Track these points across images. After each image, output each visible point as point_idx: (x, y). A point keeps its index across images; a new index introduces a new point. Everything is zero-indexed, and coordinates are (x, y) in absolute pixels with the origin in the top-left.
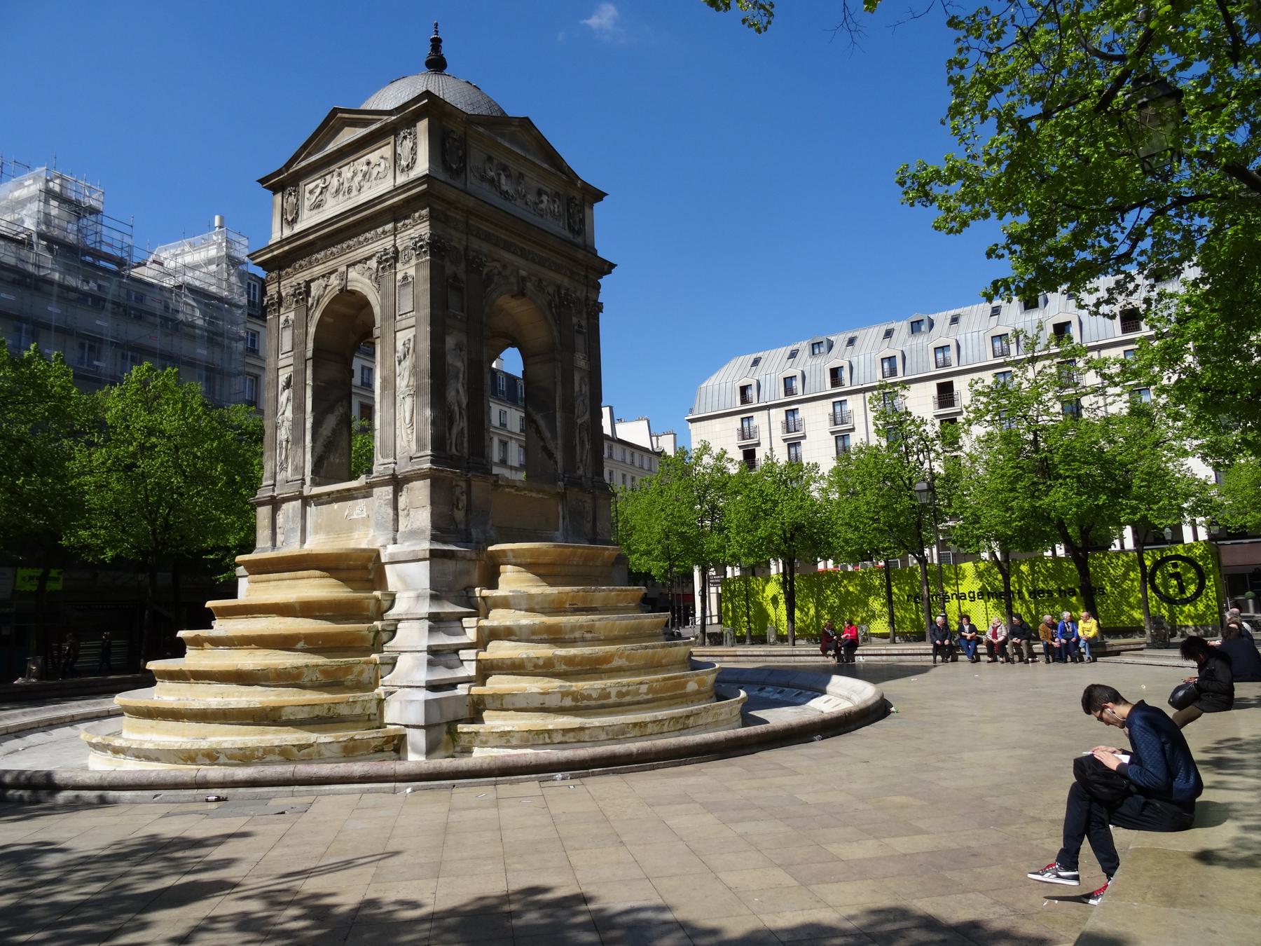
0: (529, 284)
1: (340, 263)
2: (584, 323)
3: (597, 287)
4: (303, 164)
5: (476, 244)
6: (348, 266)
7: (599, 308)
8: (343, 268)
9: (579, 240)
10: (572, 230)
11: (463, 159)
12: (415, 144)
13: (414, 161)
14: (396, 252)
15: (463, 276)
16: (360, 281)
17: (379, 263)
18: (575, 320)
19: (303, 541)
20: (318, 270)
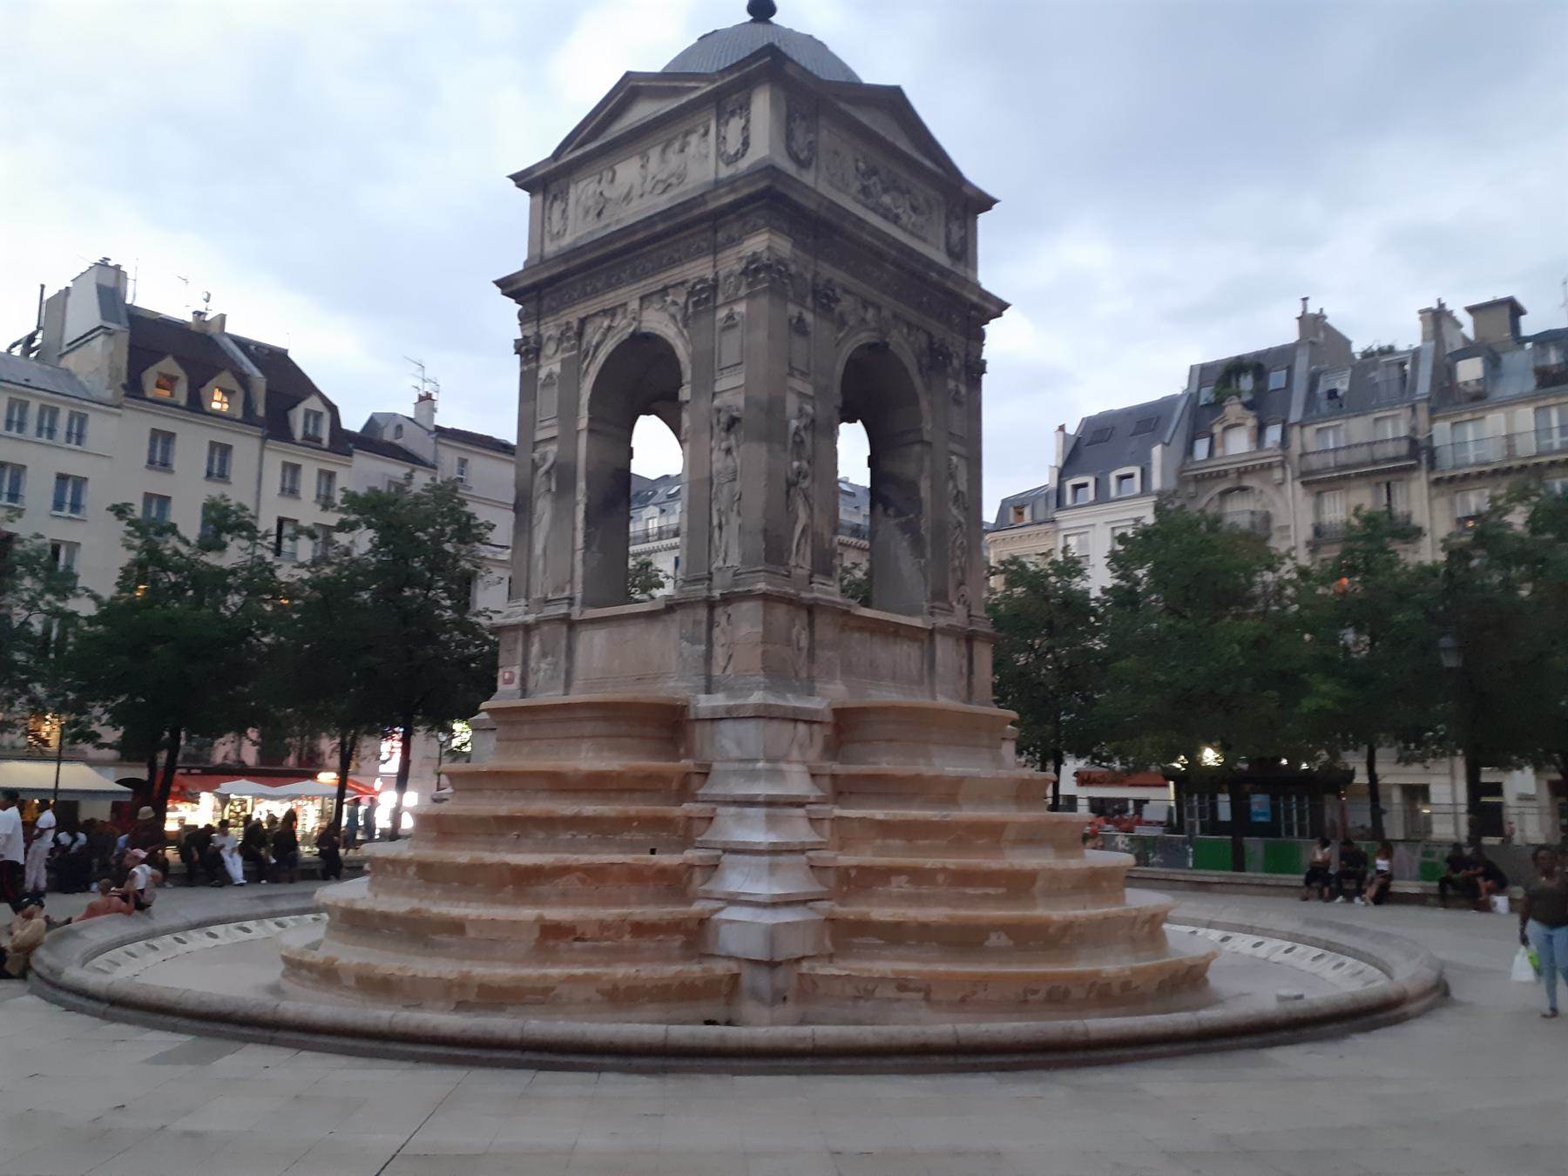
0: (895, 333)
1: (629, 295)
2: (963, 389)
3: (981, 337)
4: (571, 157)
5: (828, 271)
6: (642, 299)
7: (981, 368)
8: (634, 305)
9: (959, 269)
10: (950, 253)
11: (811, 146)
12: (748, 121)
13: (746, 143)
14: (716, 280)
15: (809, 317)
16: (658, 322)
17: (690, 294)
18: (951, 384)
19: (568, 685)
20: (594, 305)
